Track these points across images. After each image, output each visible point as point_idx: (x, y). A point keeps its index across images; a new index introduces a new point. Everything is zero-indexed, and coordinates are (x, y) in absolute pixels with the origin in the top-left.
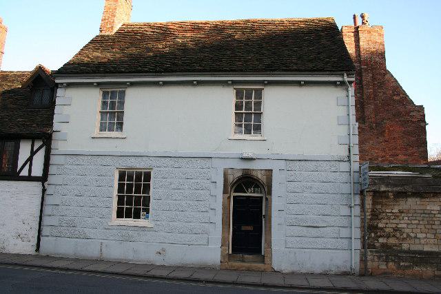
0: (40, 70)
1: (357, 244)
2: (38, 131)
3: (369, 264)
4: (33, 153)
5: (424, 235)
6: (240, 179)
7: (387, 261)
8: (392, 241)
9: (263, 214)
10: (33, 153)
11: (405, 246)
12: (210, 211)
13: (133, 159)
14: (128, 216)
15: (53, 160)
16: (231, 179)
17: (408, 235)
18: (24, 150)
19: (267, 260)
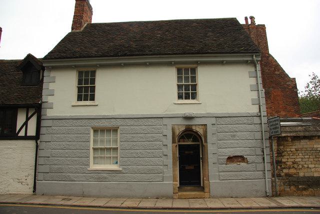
0: (30, 57)
1: (268, 175)
2: (31, 102)
3: (278, 188)
4: (28, 119)
5: (313, 166)
6: (184, 131)
7: (290, 185)
8: (292, 171)
9: (201, 156)
10: (28, 119)
11: (301, 174)
12: (164, 157)
13: (103, 121)
14: (86, 99)
15: (44, 123)
16: (177, 132)
17: (303, 166)
18: (21, 119)
19: (206, 190)
